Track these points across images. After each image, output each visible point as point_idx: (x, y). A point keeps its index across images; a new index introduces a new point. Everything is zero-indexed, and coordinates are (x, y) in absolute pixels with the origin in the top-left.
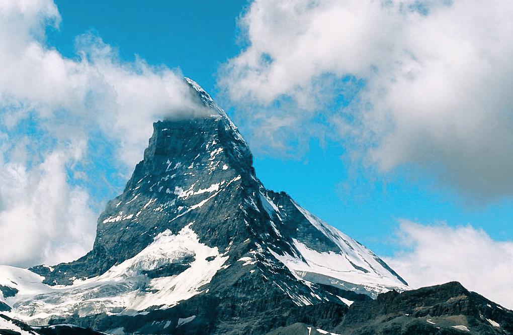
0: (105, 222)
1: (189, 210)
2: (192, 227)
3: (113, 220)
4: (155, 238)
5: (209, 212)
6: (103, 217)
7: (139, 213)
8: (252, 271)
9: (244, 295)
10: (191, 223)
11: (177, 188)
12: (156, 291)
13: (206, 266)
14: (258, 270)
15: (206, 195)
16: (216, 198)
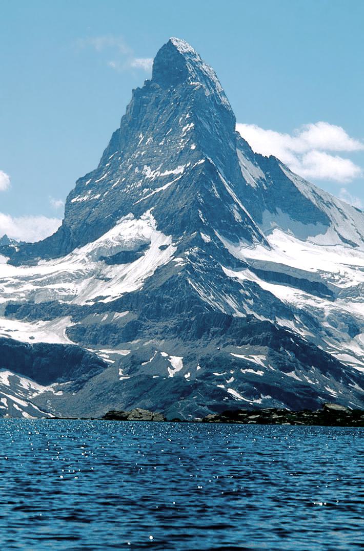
0: (73, 201)
1: (153, 193)
2: (153, 213)
3: (80, 199)
4: (118, 222)
5: (170, 198)
6: (71, 196)
7: (106, 193)
8: (179, 274)
9: (168, 297)
10: (153, 208)
11: (146, 167)
12: (108, 280)
13: (160, 253)
14: (184, 273)
15: (171, 177)
16: (179, 182)
